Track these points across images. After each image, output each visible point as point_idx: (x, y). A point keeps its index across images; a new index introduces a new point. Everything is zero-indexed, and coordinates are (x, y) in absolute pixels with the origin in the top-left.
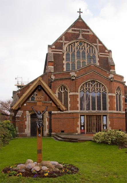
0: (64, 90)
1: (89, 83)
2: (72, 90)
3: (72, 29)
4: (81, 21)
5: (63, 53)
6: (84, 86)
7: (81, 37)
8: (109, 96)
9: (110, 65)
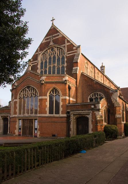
1: (26, 89)
7: (51, 43)
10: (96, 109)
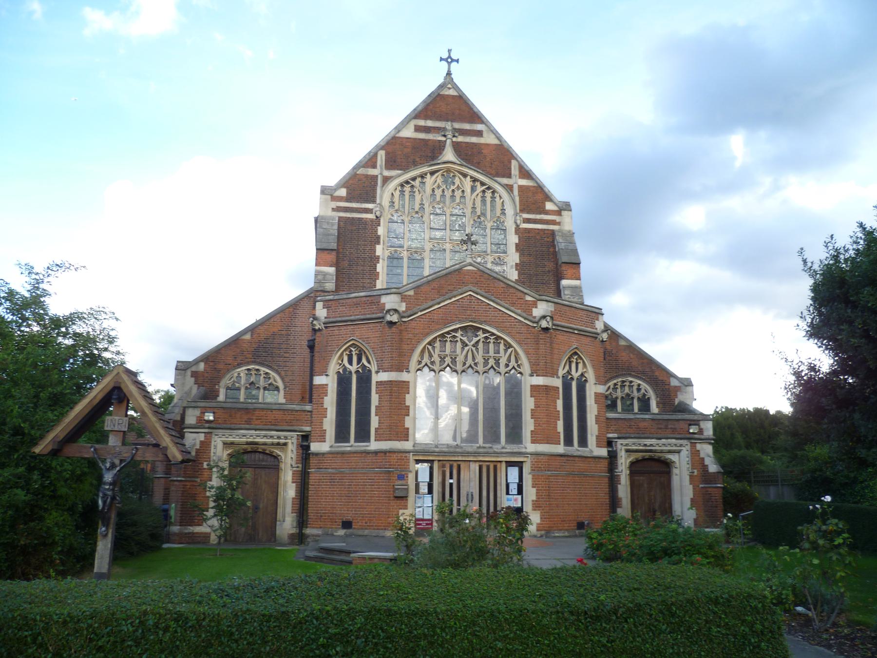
0: (358, 365)
1: (454, 337)
2: (386, 365)
3: (415, 126)
4: (452, 92)
5: (377, 217)
6: (434, 348)
7: (449, 155)
8: (535, 388)
9: (560, 262)
10: (702, 437)
